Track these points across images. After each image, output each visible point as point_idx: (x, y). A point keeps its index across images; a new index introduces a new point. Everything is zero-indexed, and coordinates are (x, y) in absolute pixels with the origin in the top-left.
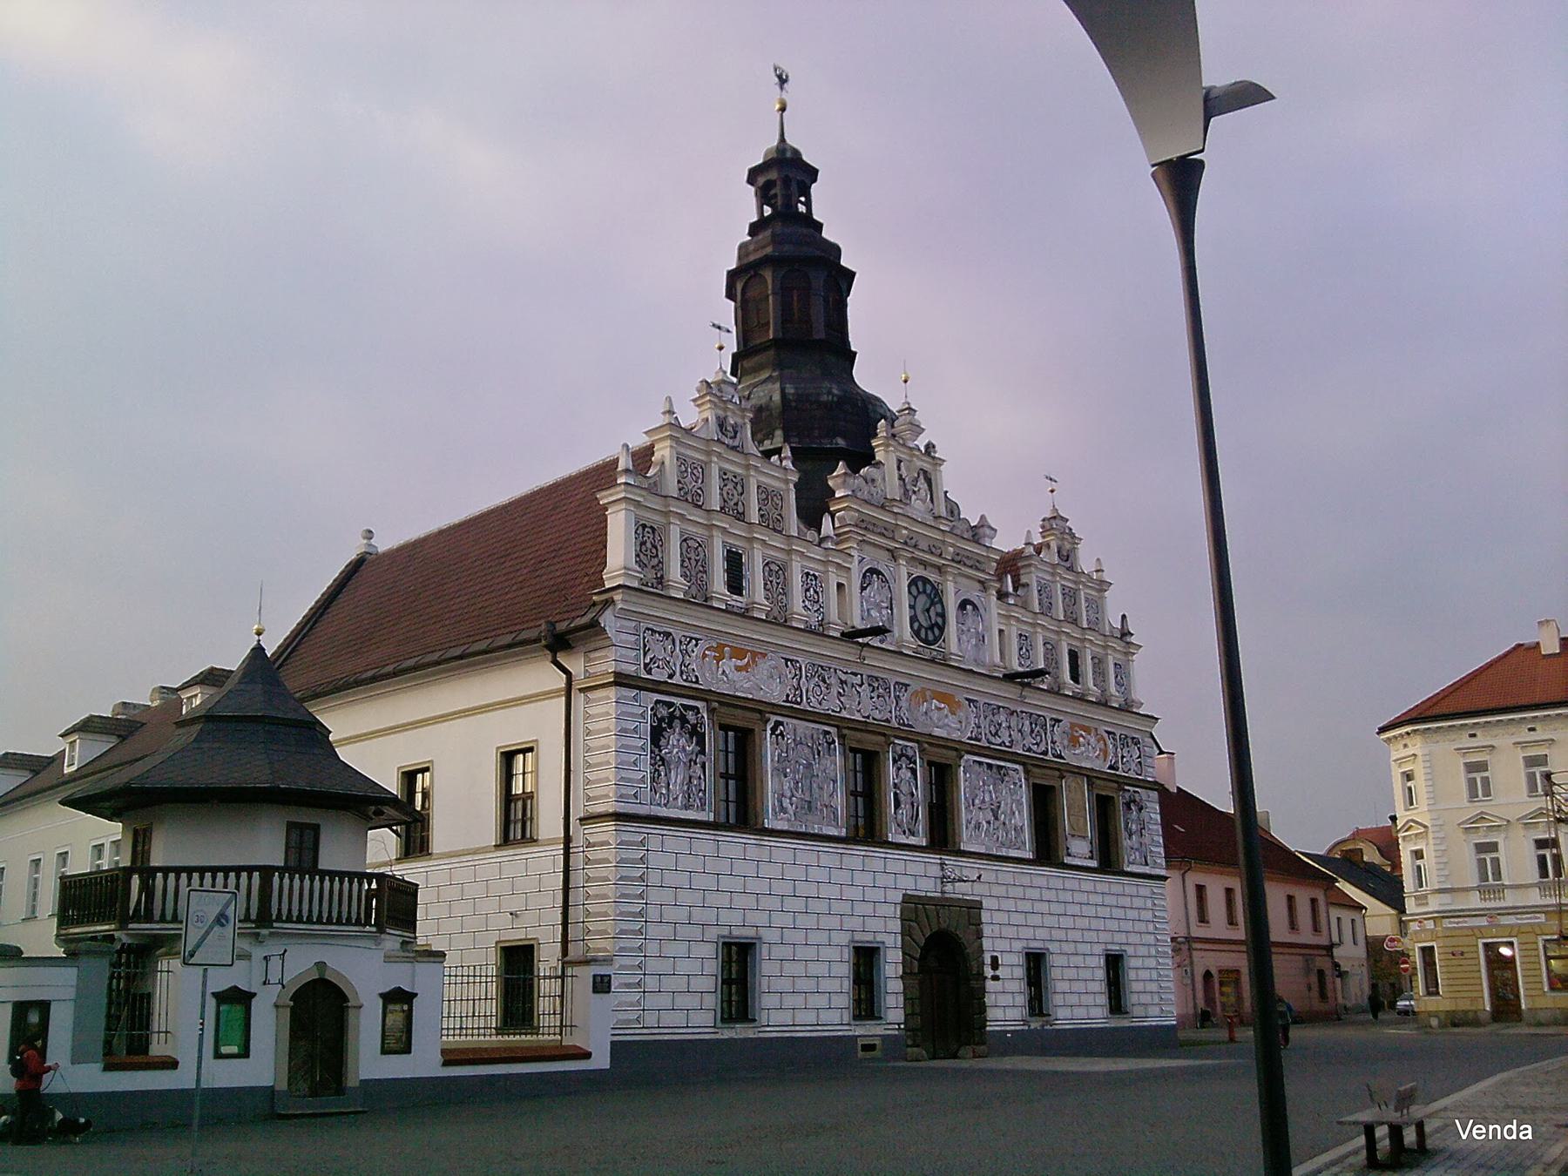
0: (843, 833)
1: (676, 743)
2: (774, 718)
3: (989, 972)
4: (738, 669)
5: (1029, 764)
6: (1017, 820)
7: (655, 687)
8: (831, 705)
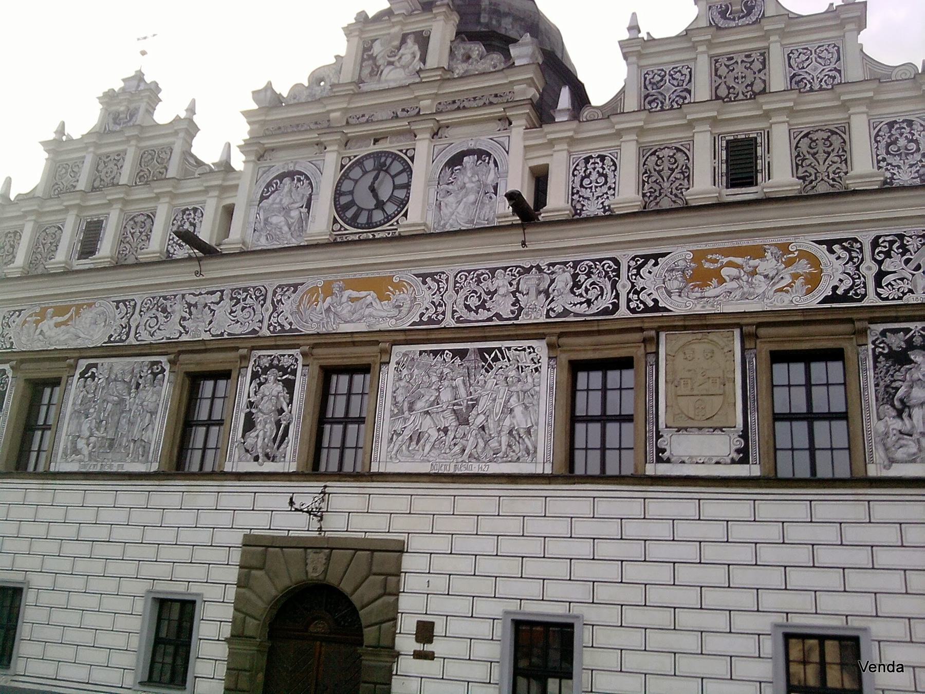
0: (154, 467)
2: (83, 364)
4: (57, 325)
6: (520, 420)
8: (170, 331)
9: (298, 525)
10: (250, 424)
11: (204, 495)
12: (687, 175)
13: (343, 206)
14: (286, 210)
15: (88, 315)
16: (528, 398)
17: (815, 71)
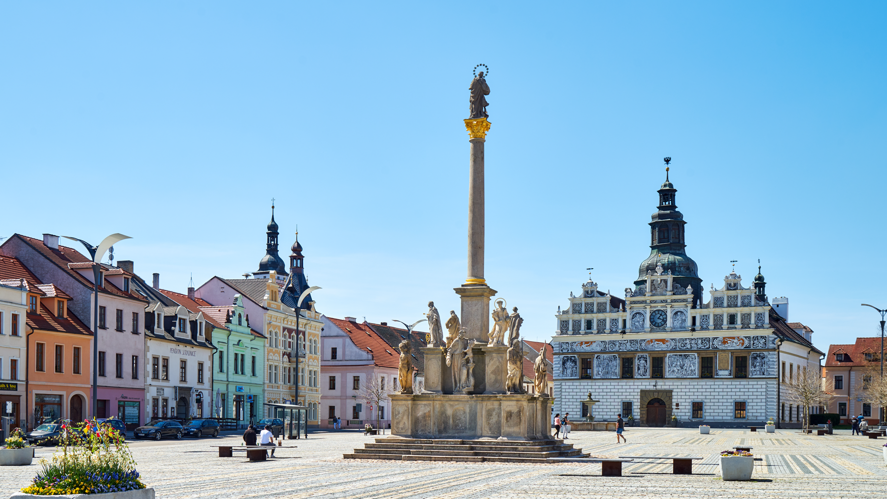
1: (569, 364)
3: (674, 407)
5: (698, 351)
6: (693, 368)
7: (563, 354)
8: (617, 348)
9: (652, 388)
10: (639, 369)
11: (630, 382)
12: (722, 321)
13: (652, 321)
15: (594, 345)
17: (746, 301)
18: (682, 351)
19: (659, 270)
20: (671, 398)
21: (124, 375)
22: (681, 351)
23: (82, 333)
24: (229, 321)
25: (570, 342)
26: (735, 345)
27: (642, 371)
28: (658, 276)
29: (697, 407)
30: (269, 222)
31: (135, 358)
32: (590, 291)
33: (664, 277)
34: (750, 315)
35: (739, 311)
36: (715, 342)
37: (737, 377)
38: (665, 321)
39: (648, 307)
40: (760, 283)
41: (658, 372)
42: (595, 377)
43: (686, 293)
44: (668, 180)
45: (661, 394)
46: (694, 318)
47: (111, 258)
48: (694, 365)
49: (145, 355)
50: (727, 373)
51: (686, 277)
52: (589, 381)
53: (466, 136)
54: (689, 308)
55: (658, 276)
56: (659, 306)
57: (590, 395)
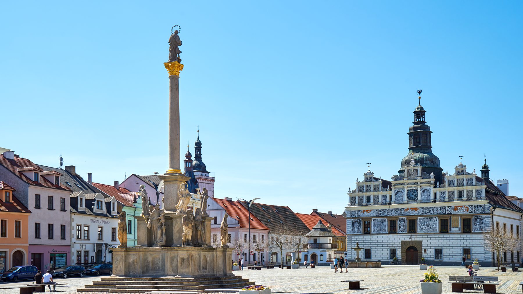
1: (356, 225)
3: (423, 252)
5: (438, 215)
6: (435, 226)
7: (352, 218)
8: (386, 214)
9: (408, 239)
10: (400, 227)
11: (395, 236)
12: (454, 195)
13: (408, 196)
14: (400, 197)
15: (372, 212)
16: (436, 224)
18: (428, 215)
19: (413, 163)
20: (421, 246)
21: (54, 237)
22: (427, 215)
23: (21, 212)
24: (135, 201)
25: (357, 210)
26: (463, 211)
27: (402, 228)
28: (412, 167)
29: (438, 252)
30: (196, 141)
31: (63, 227)
32: (369, 178)
33: (416, 168)
34: (472, 191)
35: (465, 189)
36: (449, 210)
37: (464, 232)
38: (416, 196)
39: (406, 187)
40: (485, 171)
41: (412, 229)
42: (372, 233)
43: (430, 178)
44: (420, 105)
45: (414, 243)
46: (435, 194)
47: (61, 164)
48: (436, 224)
49: (70, 224)
50: (457, 229)
51: (431, 167)
52: (369, 235)
53: (166, 74)
54: (432, 187)
55: (412, 167)
56: (413, 187)
57: (358, 245)
